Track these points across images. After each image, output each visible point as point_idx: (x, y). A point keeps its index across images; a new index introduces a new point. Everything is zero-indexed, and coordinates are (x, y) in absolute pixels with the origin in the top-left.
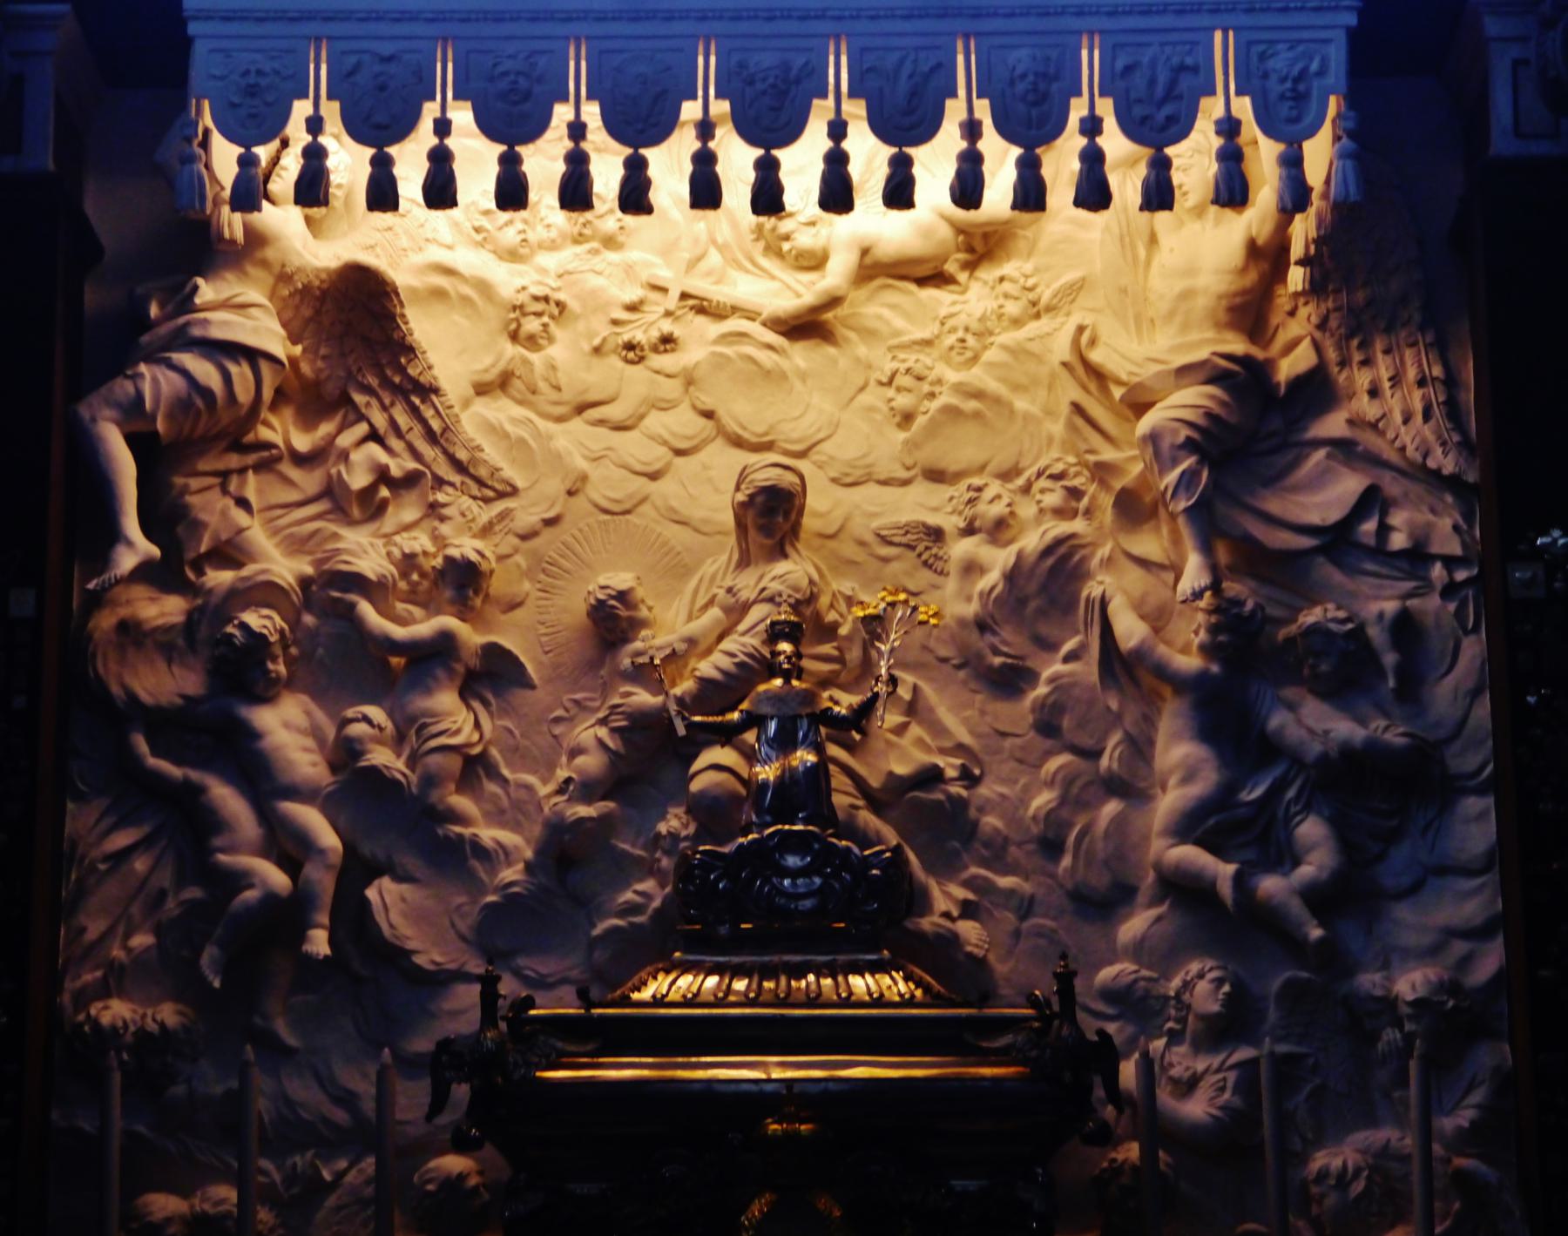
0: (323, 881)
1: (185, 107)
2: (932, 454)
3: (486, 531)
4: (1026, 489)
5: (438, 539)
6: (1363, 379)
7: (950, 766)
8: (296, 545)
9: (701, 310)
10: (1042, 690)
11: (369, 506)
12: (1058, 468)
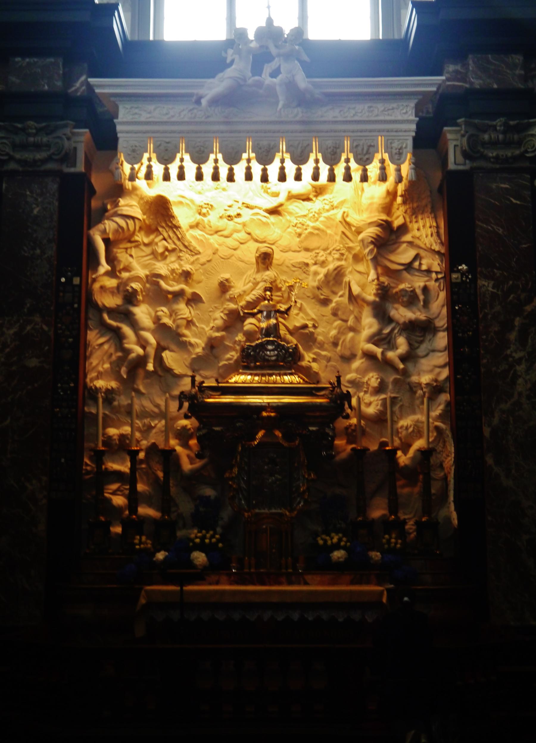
0: (151, 351)
1: (116, 155)
2: (305, 244)
3: (192, 263)
4: (330, 254)
5: (181, 265)
6: (416, 226)
7: (310, 324)
8: (145, 266)
9: (247, 207)
10: (333, 305)
11: (163, 257)
12: (338, 248)
